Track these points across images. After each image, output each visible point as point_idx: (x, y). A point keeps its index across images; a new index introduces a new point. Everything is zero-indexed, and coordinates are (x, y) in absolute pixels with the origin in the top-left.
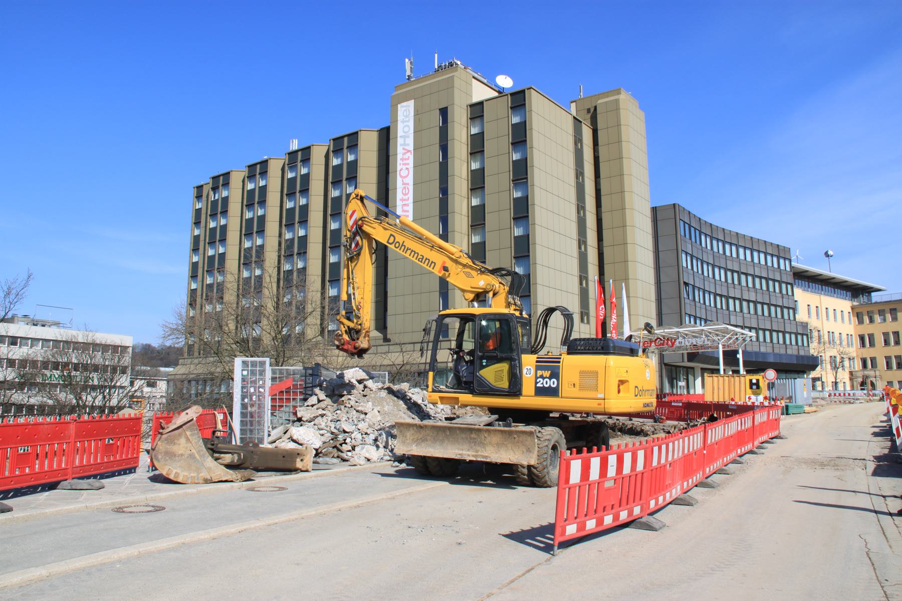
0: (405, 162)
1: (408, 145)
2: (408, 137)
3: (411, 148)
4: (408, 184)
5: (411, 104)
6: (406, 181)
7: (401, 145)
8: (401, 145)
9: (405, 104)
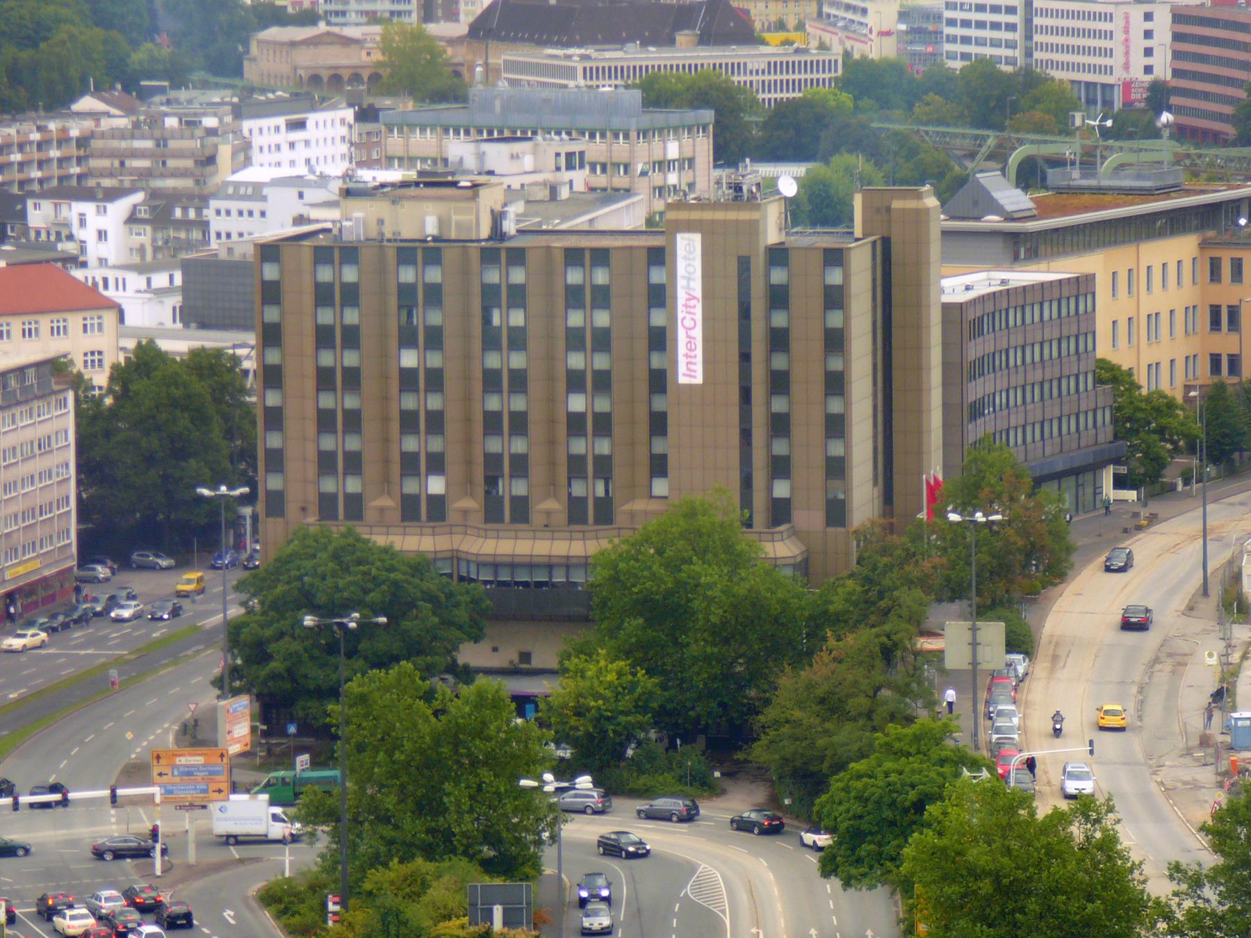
0: (689, 310)
1: (694, 290)
2: (694, 280)
3: (698, 293)
4: (694, 338)
5: (697, 238)
6: (692, 333)
7: (683, 287)
8: (683, 287)
9: (686, 235)
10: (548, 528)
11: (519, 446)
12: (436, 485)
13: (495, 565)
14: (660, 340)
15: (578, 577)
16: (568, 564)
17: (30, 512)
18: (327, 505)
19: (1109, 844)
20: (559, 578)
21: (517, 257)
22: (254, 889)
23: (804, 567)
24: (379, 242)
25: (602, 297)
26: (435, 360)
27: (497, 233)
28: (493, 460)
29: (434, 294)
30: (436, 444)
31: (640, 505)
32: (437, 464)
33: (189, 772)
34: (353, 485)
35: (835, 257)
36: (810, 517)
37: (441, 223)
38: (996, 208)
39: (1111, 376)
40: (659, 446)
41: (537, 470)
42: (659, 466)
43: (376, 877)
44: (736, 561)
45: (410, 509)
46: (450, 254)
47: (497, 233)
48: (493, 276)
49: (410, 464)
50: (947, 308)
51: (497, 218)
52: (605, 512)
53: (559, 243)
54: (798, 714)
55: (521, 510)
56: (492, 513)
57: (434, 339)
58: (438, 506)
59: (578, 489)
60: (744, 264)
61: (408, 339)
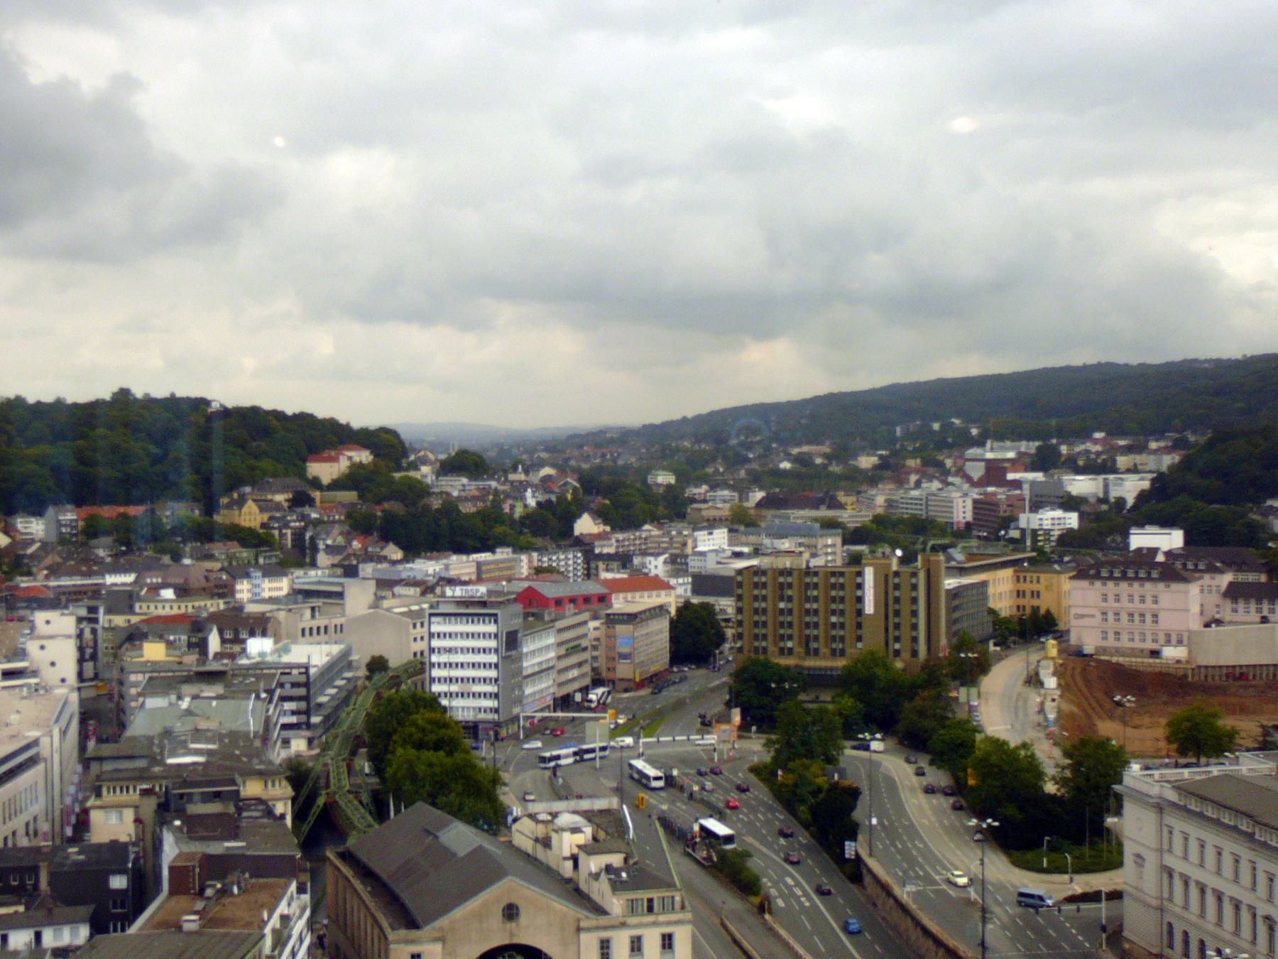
10: (825, 657)
11: (815, 632)
12: (790, 644)
13: (809, 669)
14: (860, 600)
15: (834, 673)
16: (831, 669)
17: (657, 651)
18: (756, 649)
19: (1033, 756)
20: (829, 673)
21: (816, 574)
22: (747, 766)
23: (904, 670)
24: (774, 570)
25: (842, 587)
26: (790, 606)
27: (808, 567)
28: (808, 637)
29: (790, 586)
30: (789, 631)
31: (853, 651)
32: (790, 638)
33: (724, 731)
34: (764, 644)
35: (914, 575)
36: (906, 655)
37: (792, 564)
38: (955, 560)
39: (992, 612)
40: (859, 632)
41: (822, 640)
42: (859, 639)
43: (791, 765)
44: (887, 668)
45: (782, 651)
46: (795, 574)
47: (808, 567)
48: (808, 580)
49: (782, 637)
50: (948, 591)
51: (808, 562)
52: (842, 653)
53: (830, 570)
54: (911, 716)
55: (816, 652)
56: (808, 652)
57: (790, 599)
58: (790, 651)
59: (834, 646)
60: (886, 576)
61: (782, 599)
